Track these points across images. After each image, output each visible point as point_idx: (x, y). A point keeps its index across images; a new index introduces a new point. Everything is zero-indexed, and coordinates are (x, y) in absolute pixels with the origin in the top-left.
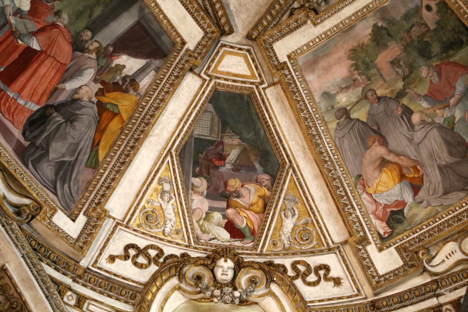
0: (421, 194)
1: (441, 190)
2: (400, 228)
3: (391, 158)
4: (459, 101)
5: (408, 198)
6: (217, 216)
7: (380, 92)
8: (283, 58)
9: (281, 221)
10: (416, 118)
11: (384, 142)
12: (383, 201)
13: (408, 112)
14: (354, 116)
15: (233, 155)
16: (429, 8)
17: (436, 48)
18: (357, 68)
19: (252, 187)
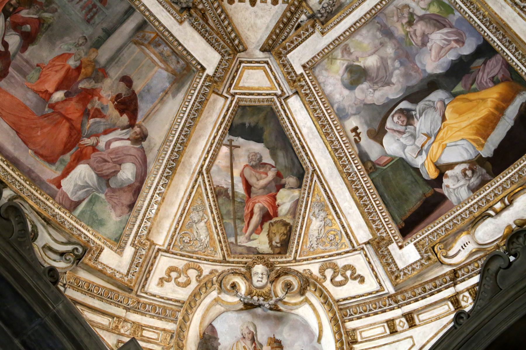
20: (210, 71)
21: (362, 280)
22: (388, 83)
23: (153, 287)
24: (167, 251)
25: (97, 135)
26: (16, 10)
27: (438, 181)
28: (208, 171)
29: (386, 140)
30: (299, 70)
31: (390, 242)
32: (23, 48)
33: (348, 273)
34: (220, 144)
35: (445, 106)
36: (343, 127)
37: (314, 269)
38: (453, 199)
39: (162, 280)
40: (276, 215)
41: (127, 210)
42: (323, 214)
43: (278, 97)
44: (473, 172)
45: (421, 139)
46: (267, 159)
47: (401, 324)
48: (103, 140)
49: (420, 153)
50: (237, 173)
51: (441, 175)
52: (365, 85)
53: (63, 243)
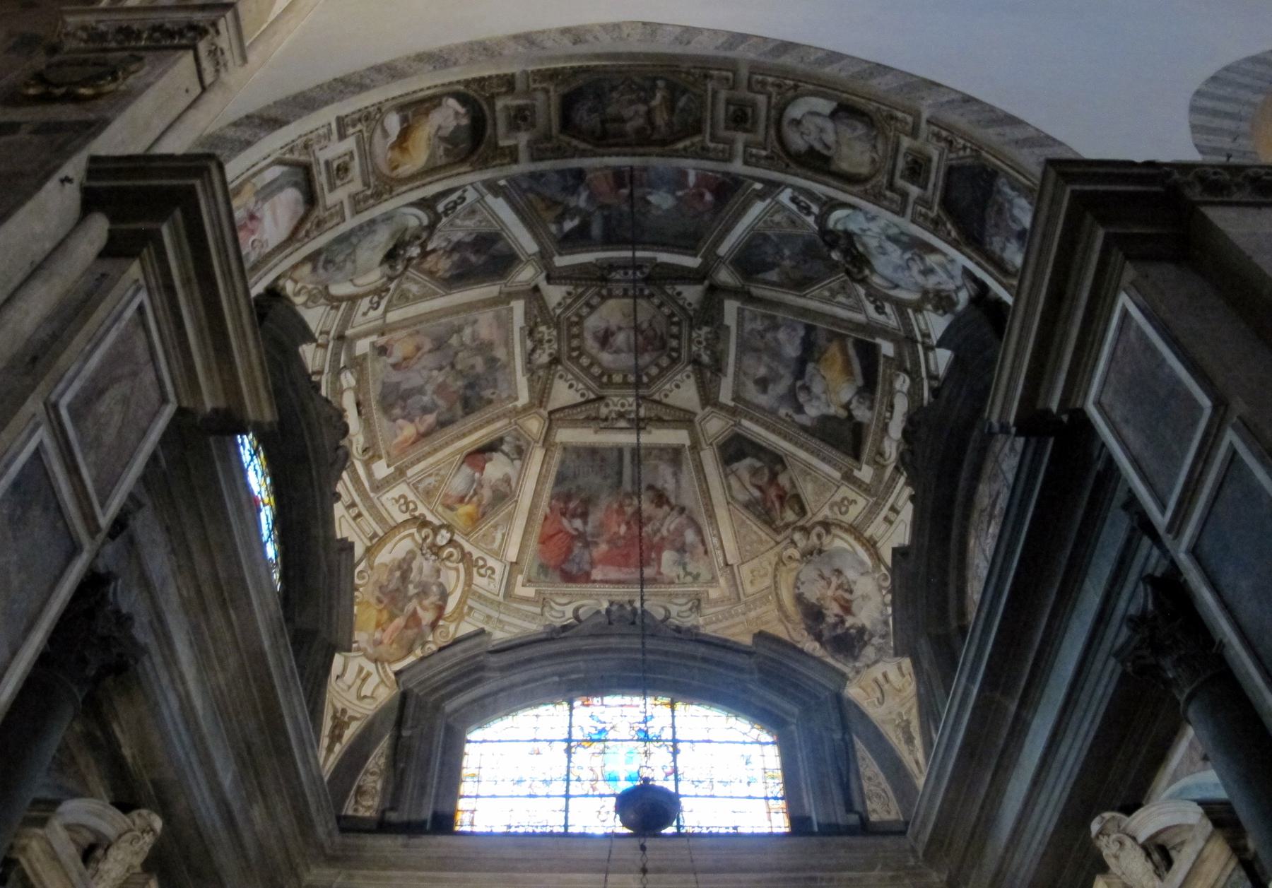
0: (390, 369)
1: (386, 380)
2: (376, 352)
3: (419, 354)
4: (433, 399)
5: (392, 360)
6: (444, 244)
7: (460, 355)
8: (514, 304)
9: (416, 282)
10: (435, 373)
11: (430, 351)
12: (396, 345)
13: (440, 368)
14: (455, 336)
15: (473, 258)
16: (493, 393)
17: (469, 393)
18: (481, 344)
19: (447, 267)
20: (688, 443)
21: (854, 502)
22: (782, 377)
23: (750, 589)
24: (743, 563)
25: (659, 530)
26: (567, 509)
27: (850, 417)
28: (732, 497)
29: (807, 409)
30: (732, 404)
31: (852, 471)
32: (585, 523)
33: (846, 502)
34: (726, 476)
35: (818, 370)
36: (780, 418)
37: (825, 512)
38: (865, 420)
39: (752, 582)
40: (786, 493)
41: (705, 557)
42: (808, 478)
43: (735, 425)
44: (863, 398)
45: (823, 397)
46: (758, 464)
47: (892, 516)
48: (664, 532)
49: (829, 406)
50: (749, 486)
51: (849, 411)
52: (771, 387)
53: (686, 603)
